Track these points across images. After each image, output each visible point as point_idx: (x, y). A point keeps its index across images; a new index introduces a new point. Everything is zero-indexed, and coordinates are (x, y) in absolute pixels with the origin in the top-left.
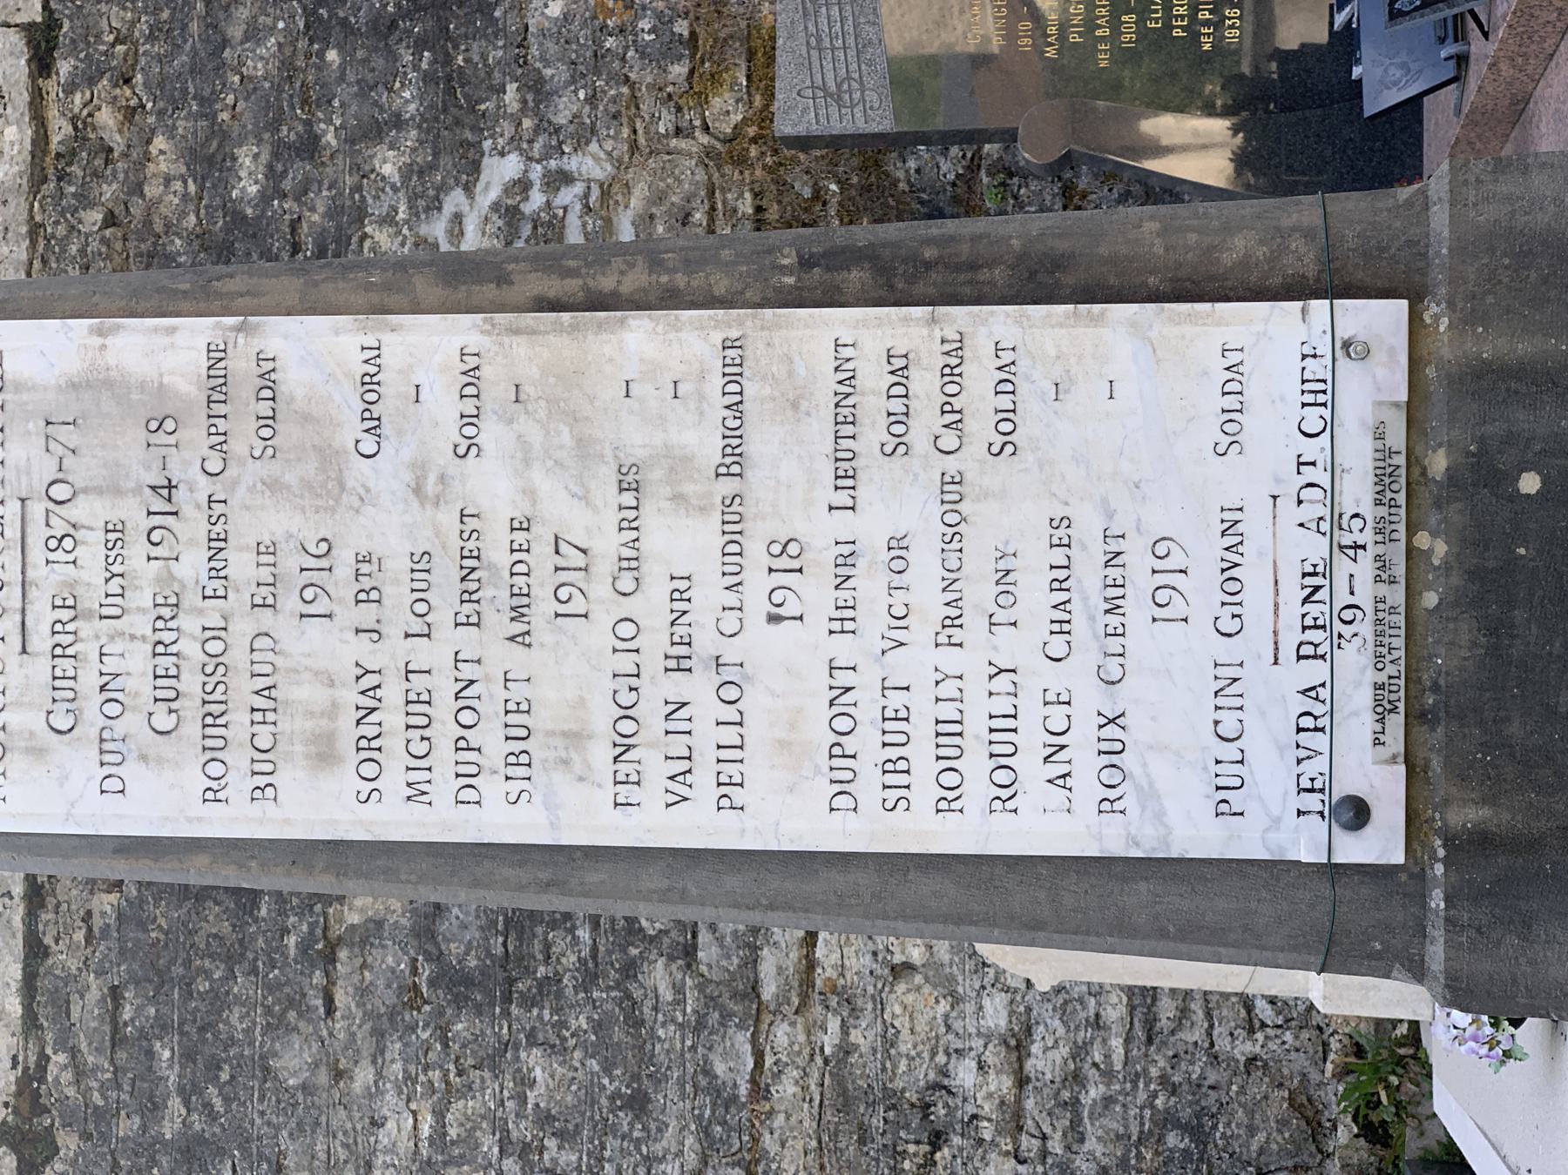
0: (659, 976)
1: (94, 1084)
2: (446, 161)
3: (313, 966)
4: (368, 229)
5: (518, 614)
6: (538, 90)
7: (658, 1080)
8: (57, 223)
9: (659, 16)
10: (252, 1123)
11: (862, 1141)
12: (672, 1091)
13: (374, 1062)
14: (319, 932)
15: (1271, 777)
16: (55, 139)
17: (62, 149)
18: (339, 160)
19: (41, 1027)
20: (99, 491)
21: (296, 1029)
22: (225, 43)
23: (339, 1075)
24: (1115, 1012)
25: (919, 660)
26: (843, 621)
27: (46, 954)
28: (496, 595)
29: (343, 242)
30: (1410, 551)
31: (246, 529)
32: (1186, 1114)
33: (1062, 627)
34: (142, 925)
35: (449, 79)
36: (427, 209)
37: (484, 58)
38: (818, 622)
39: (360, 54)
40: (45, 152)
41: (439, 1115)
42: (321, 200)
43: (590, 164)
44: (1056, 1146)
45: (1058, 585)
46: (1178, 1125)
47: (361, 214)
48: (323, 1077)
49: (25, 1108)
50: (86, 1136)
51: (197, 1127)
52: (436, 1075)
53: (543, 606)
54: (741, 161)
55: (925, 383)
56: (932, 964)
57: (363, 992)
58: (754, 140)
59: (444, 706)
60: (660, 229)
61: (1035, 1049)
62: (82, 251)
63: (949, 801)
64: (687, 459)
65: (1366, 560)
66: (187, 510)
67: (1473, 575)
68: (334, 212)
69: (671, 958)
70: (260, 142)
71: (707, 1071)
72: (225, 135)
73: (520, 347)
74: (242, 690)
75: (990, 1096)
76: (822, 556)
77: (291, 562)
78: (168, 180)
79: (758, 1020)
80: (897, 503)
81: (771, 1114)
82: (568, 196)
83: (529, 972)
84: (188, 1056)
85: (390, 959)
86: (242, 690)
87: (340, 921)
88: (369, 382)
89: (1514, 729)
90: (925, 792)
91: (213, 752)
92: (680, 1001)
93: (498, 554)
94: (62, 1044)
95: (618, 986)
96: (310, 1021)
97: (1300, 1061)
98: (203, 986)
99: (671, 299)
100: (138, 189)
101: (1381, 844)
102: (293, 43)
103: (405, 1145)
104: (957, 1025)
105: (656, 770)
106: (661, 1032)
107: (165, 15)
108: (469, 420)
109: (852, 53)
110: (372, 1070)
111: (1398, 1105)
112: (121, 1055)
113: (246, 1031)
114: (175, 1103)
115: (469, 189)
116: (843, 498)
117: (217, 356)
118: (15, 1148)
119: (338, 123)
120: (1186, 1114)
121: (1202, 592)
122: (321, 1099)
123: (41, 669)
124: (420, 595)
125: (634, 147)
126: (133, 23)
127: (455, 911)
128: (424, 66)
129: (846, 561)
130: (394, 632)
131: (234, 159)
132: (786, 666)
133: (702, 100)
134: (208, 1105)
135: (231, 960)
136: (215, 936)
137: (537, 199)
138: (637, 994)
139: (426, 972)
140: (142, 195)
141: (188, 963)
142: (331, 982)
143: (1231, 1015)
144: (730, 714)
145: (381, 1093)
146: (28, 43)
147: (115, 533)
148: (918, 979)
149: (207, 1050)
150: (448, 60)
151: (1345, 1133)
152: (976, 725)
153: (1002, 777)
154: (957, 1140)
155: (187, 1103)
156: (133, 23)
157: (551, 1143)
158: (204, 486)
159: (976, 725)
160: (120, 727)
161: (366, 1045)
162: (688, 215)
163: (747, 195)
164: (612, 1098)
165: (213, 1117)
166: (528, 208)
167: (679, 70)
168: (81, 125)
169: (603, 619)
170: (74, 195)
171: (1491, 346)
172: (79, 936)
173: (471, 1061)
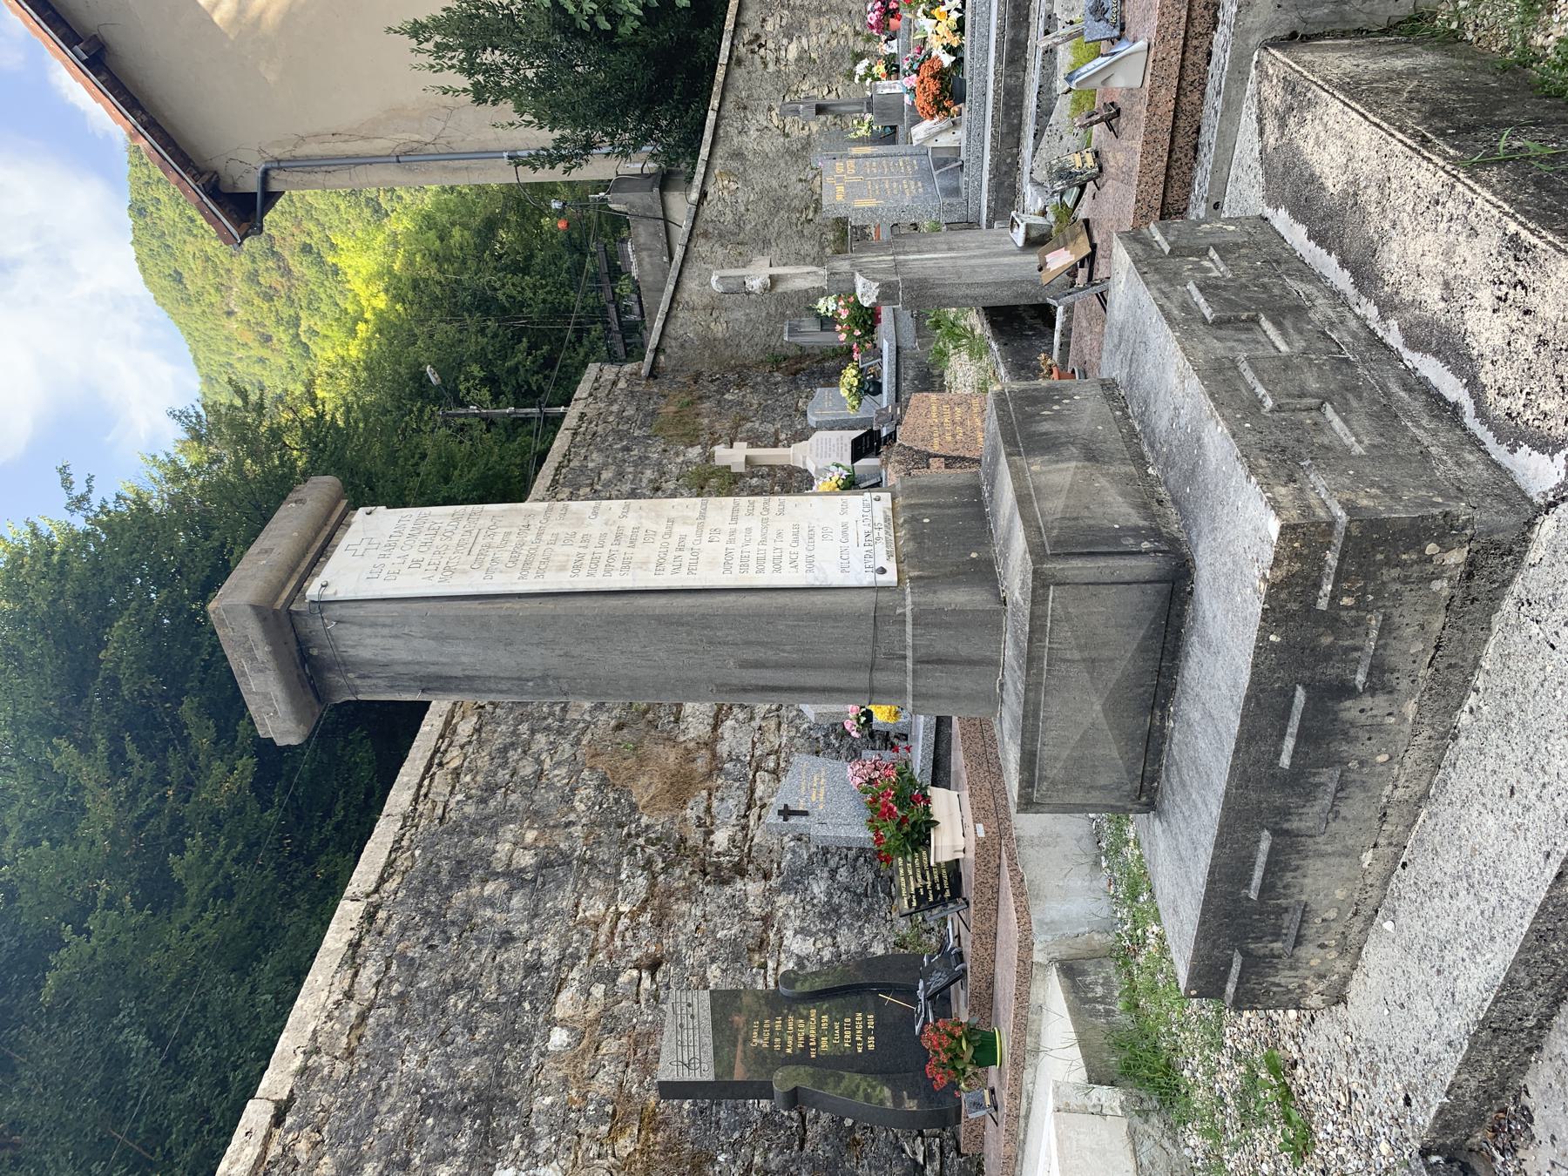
6: (531, 1137)
22: (377, 1113)
70: (379, 1159)
72: (362, 1157)
101: (891, 578)
133: (614, 1140)
150: (489, 1124)
159: (769, 557)
167: (604, 1129)
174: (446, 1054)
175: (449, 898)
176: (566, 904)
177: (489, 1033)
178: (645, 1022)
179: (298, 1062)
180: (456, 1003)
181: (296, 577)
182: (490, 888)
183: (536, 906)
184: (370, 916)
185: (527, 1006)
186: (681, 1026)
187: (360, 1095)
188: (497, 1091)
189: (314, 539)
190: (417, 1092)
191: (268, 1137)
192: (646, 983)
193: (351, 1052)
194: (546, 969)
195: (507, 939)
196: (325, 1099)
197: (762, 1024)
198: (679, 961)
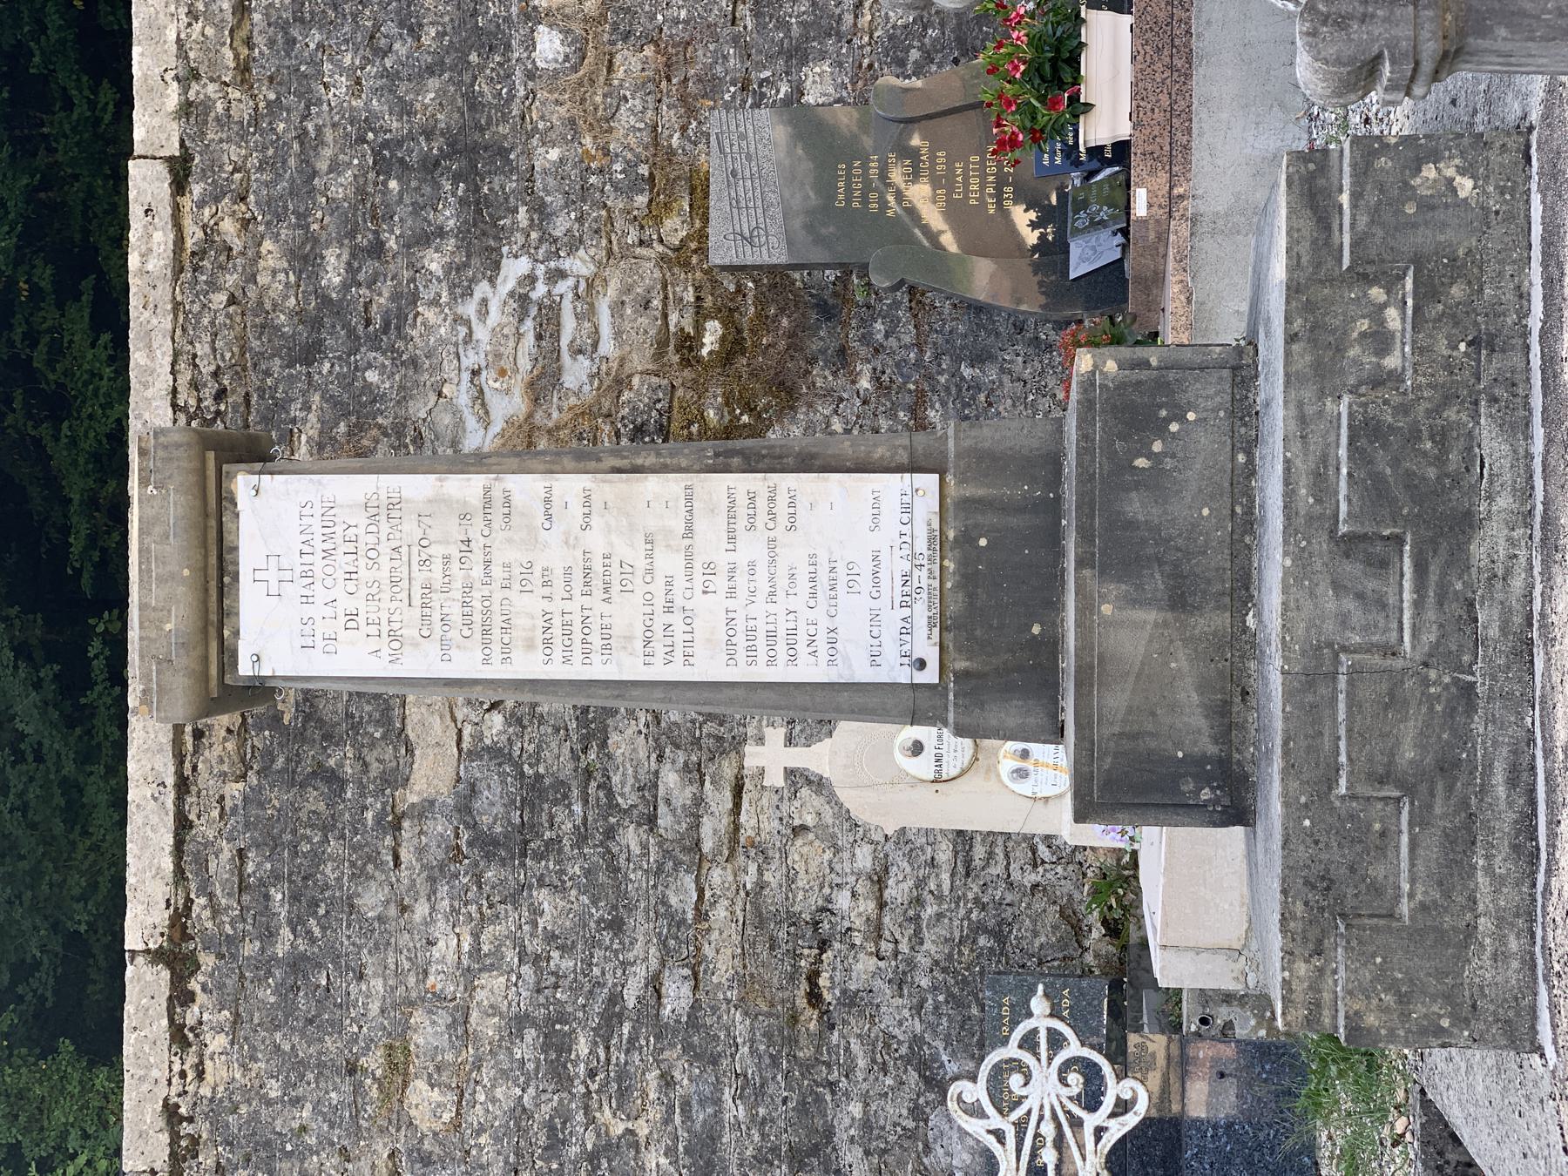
0: (631, 837)
1: (227, 919)
2: (475, 261)
3: (385, 833)
4: (420, 309)
5: (606, 591)
6: (541, 211)
7: (630, 909)
8: (193, 302)
9: (627, 162)
10: (342, 944)
11: (772, 948)
12: (640, 917)
13: (429, 899)
14: (389, 808)
15: (891, 652)
16: (189, 244)
17: (196, 248)
18: (399, 260)
19: (187, 879)
20: (440, 542)
21: (373, 877)
22: (315, 173)
23: (404, 909)
24: (944, 855)
25: (760, 608)
26: (731, 593)
27: (191, 827)
28: (597, 583)
30: (941, 567)
31: (498, 558)
32: (991, 923)
33: (813, 595)
34: (261, 805)
35: (477, 203)
36: (463, 295)
37: (503, 188)
38: (722, 594)
39: (414, 184)
40: (182, 249)
41: (476, 936)
42: (386, 289)
43: (579, 265)
44: (904, 947)
45: (812, 580)
46: (986, 931)
47: (414, 298)
48: (393, 911)
49: (177, 935)
50: (220, 956)
51: (302, 948)
52: (473, 908)
53: (616, 588)
54: (686, 265)
55: (762, 503)
56: (821, 826)
57: (421, 851)
58: (695, 251)
59: (577, 627)
60: (629, 311)
61: (891, 882)
62: (212, 323)
63: (772, 661)
64: (671, 532)
65: (925, 571)
66: (475, 550)
67: (963, 576)
68: (396, 296)
69: (639, 825)
71: (664, 902)
72: (316, 241)
73: (607, 487)
74: (497, 620)
75: (860, 915)
76: (723, 568)
77: (517, 570)
78: (274, 272)
79: (700, 867)
80: (751, 548)
81: (709, 930)
82: (563, 287)
83: (539, 835)
84: (295, 898)
85: (440, 827)
86: (497, 620)
87: (404, 801)
88: (547, 501)
89: (978, 633)
90: (762, 657)
91: (486, 645)
93: (598, 567)
95: (602, 844)
96: (383, 871)
97: (1068, 886)
98: (305, 847)
100: (253, 279)
101: (930, 676)
102: (365, 175)
103: (451, 958)
104: (838, 867)
106: (632, 876)
107: (270, 152)
108: (587, 515)
109: (760, 211)
110: (427, 906)
111: (1124, 908)
112: (246, 898)
113: (338, 879)
114: (286, 932)
115: (492, 281)
116: (731, 547)
117: (487, 490)
118: (169, 965)
119: (398, 233)
120: (991, 923)
121: (865, 582)
122: (391, 926)
123: (417, 612)
124: (568, 583)
125: (610, 253)
126: (246, 157)
127: (486, 793)
128: (460, 193)
129: (732, 570)
130: (557, 598)
131: (323, 258)
132: (710, 612)
133: (658, 221)
134: (309, 932)
135: (325, 829)
136: (314, 812)
137: (541, 290)
138: (615, 850)
139: (465, 836)
140: (256, 283)
141: (294, 832)
142: (398, 844)
143: (1021, 855)
144: (688, 629)
145: (433, 921)
146: (170, 171)
147: (447, 559)
148: (811, 836)
149: (309, 893)
150: (477, 189)
151: (1097, 932)
152: (782, 633)
153: (792, 652)
154: (837, 945)
155: (294, 931)
156: (246, 157)
157: (555, 954)
158: (482, 541)
159: (782, 633)
160: (449, 635)
161: (423, 889)
162: (649, 301)
163: (690, 289)
164: (598, 922)
165: (313, 941)
166: (534, 295)
167: (641, 200)
168: (209, 231)
169: (639, 592)
170: (206, 282)
171: (969, 491)
172: (215, 813)
173: (498, 898)
174: (384, 73)
177: (441, 35)
178: (676, 21)
179: (173, 97)
181: (213, 632)
186: (734, 173)
187: (282, 147)
188: (477, 136)
189: (206, 557)
190: (362, 140)
191: (177, 209)
193: (243, 68)
196: (234, 153)
197: (850, 168)
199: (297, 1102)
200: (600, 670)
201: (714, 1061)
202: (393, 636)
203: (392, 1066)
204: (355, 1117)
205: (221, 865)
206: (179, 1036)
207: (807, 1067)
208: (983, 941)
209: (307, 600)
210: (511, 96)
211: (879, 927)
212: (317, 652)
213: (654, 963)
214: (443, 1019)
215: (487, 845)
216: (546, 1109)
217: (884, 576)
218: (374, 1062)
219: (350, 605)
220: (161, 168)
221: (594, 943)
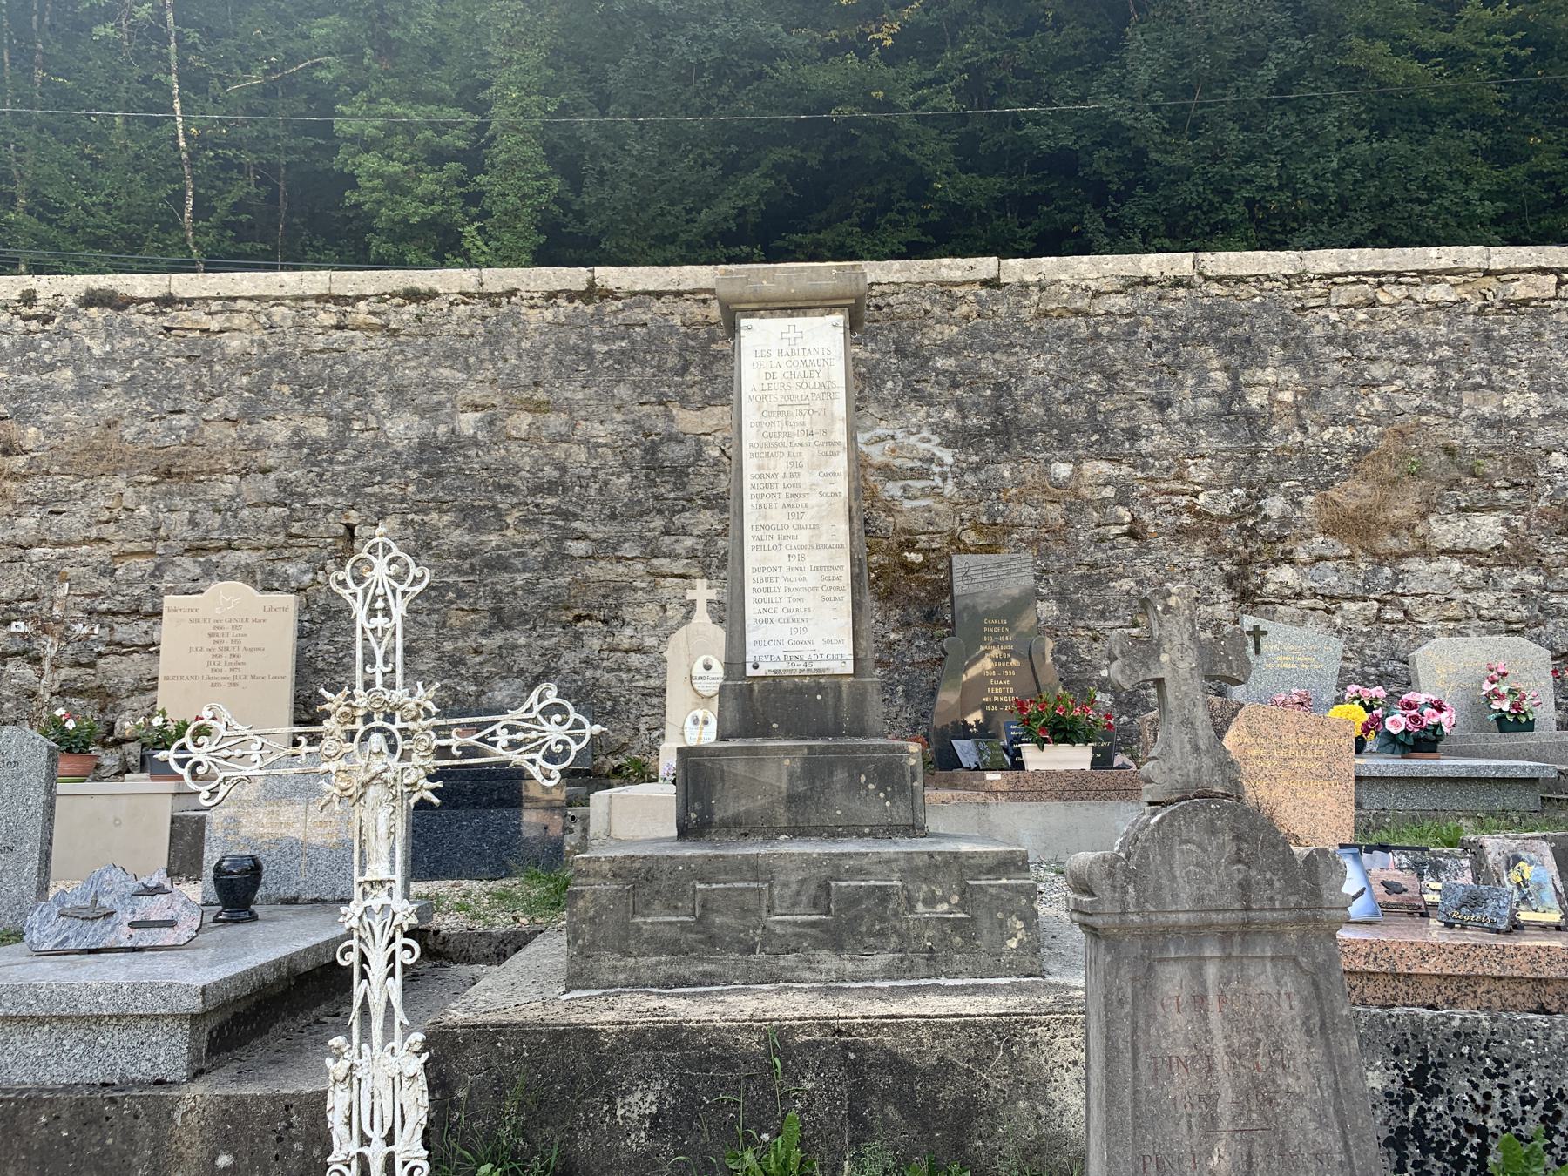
0: (658, 522)
6: (977, 468)
7: (621, 523)
15: (762, 651)
24: (653, 683)
25: (782, 584)
26: (789, 569)
28: (793, 501)
29: (920, 399)
31: (805, 451)
41: (606, 445)
42: (935, 390)
43: (950, 488)
44: (605, 663)
47: (930, 405)
48: (617, 402)
54: (951, 543)
55: (836, 583)
56: (667, 619)
57: (648, 416)
68: (931, 395)
74: (772, 451)
80: (812, 579)
82: (938, 481)
84: (623, 353)
85: (661, 425)
86: (772, 451)
90: (757, 586)
92: (650, 530)
94: (626, 306)
97: (638, 747)
99: (852, 534)
101: (750, 672)
103: (594, 433)
105: (759, 534)
114: (606, 348)
118: (587, 290)
132: (781, 558)
133: (973, 528)
135: (658, 367)
137: (937, 469)
139: (656, 438)
143: (654, 722)
147: (803, 424)
151: (616, 763)
165: (601, 362)
167: (984, 520)
168: (962, 299)
171: (845, 689)
174: (1046, 386)
175: (1205, 343)
176: (1203, 447)
179: (1030, 278)
180: (1094, 382)
182: (1218, 376)
183: (1201, 421)
184: (1177, 283)
185: (1096, 437)
187: (1006, 335)
191: (973, 282)
192: (1115, 530)
193: (1046, 314)
194: (1132, 446)
195: (1161, 405)
196: (1003, 311)
198: (1139, 554)
199: (519, 356)
200: (748, 503)
201: (545, 568)
202: (763, 397)
203: (539, 405)
204: (512, 386)
205: (639, 315)
206: (551, 296)
207: (543, 615)
208: (609, 704)
209: (780, 352)
210: (1036, 451)
211: (615, 650)
212: (753, 358)
213: (594, 536)
214: (563, 430)
215: (652, 450)
216: (518, 483)
217: (800, 647)
218: (541, 395)
219: (779, 372)
220: (994, 274)
221: (603, 506)
